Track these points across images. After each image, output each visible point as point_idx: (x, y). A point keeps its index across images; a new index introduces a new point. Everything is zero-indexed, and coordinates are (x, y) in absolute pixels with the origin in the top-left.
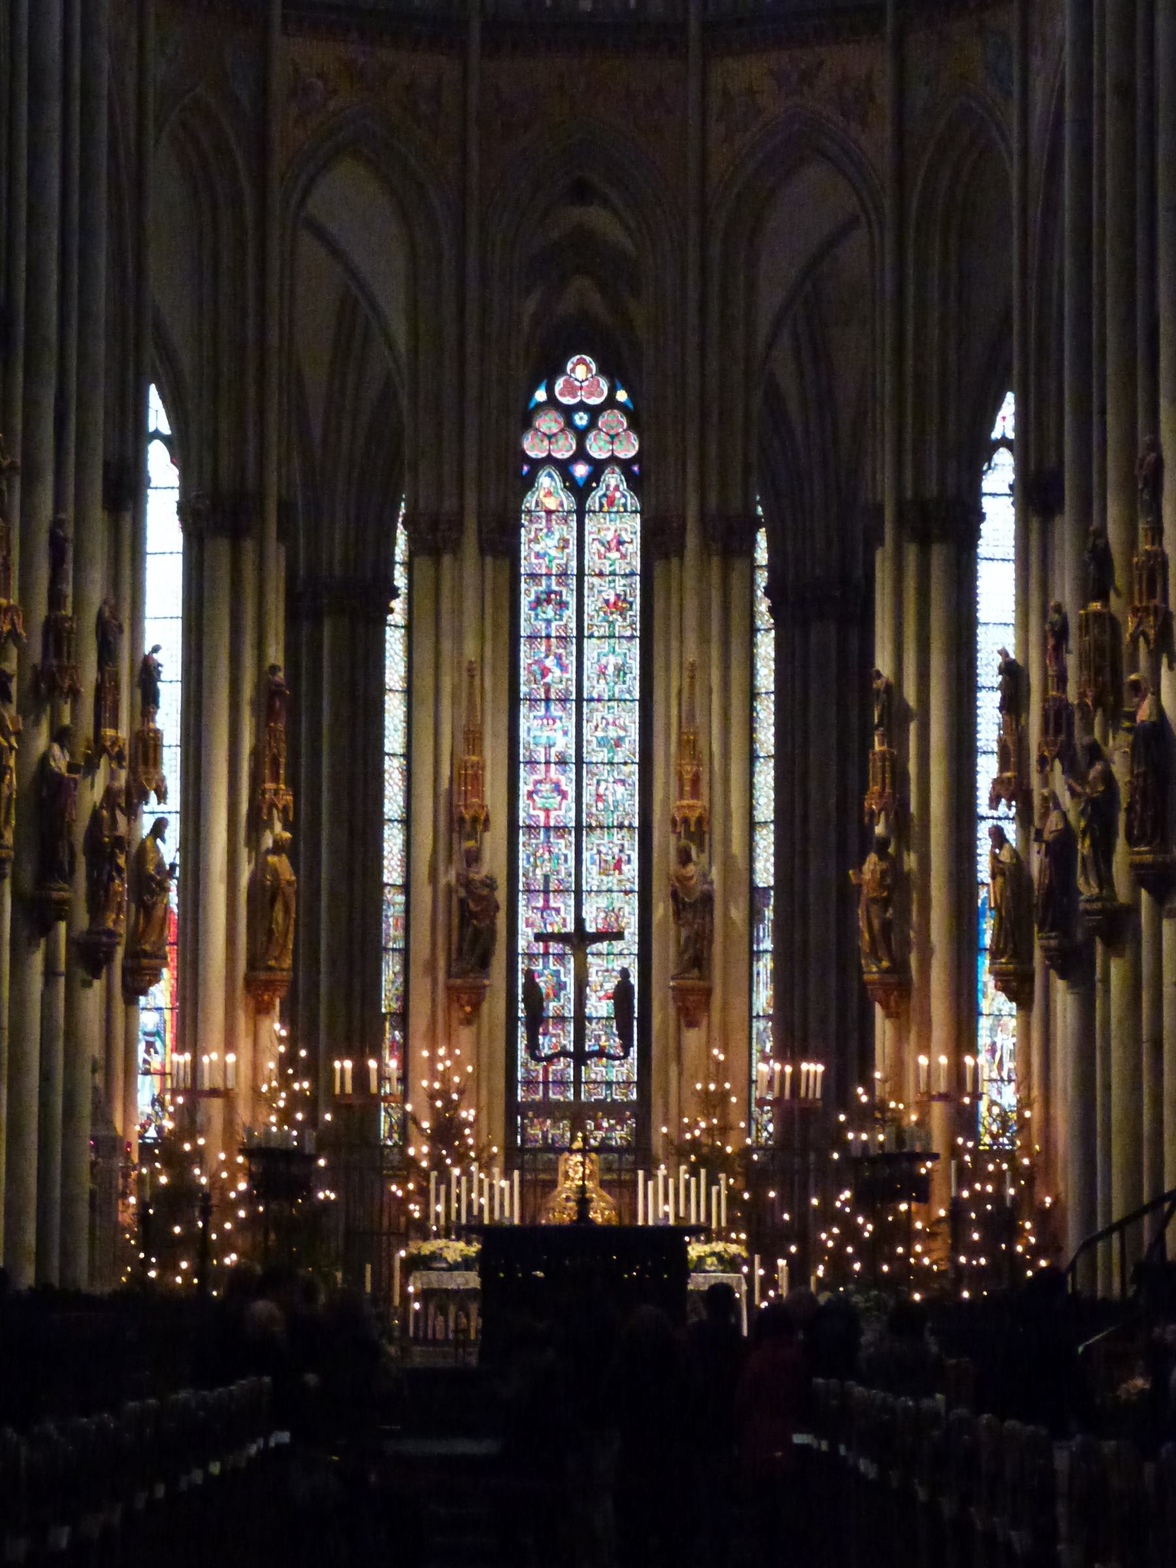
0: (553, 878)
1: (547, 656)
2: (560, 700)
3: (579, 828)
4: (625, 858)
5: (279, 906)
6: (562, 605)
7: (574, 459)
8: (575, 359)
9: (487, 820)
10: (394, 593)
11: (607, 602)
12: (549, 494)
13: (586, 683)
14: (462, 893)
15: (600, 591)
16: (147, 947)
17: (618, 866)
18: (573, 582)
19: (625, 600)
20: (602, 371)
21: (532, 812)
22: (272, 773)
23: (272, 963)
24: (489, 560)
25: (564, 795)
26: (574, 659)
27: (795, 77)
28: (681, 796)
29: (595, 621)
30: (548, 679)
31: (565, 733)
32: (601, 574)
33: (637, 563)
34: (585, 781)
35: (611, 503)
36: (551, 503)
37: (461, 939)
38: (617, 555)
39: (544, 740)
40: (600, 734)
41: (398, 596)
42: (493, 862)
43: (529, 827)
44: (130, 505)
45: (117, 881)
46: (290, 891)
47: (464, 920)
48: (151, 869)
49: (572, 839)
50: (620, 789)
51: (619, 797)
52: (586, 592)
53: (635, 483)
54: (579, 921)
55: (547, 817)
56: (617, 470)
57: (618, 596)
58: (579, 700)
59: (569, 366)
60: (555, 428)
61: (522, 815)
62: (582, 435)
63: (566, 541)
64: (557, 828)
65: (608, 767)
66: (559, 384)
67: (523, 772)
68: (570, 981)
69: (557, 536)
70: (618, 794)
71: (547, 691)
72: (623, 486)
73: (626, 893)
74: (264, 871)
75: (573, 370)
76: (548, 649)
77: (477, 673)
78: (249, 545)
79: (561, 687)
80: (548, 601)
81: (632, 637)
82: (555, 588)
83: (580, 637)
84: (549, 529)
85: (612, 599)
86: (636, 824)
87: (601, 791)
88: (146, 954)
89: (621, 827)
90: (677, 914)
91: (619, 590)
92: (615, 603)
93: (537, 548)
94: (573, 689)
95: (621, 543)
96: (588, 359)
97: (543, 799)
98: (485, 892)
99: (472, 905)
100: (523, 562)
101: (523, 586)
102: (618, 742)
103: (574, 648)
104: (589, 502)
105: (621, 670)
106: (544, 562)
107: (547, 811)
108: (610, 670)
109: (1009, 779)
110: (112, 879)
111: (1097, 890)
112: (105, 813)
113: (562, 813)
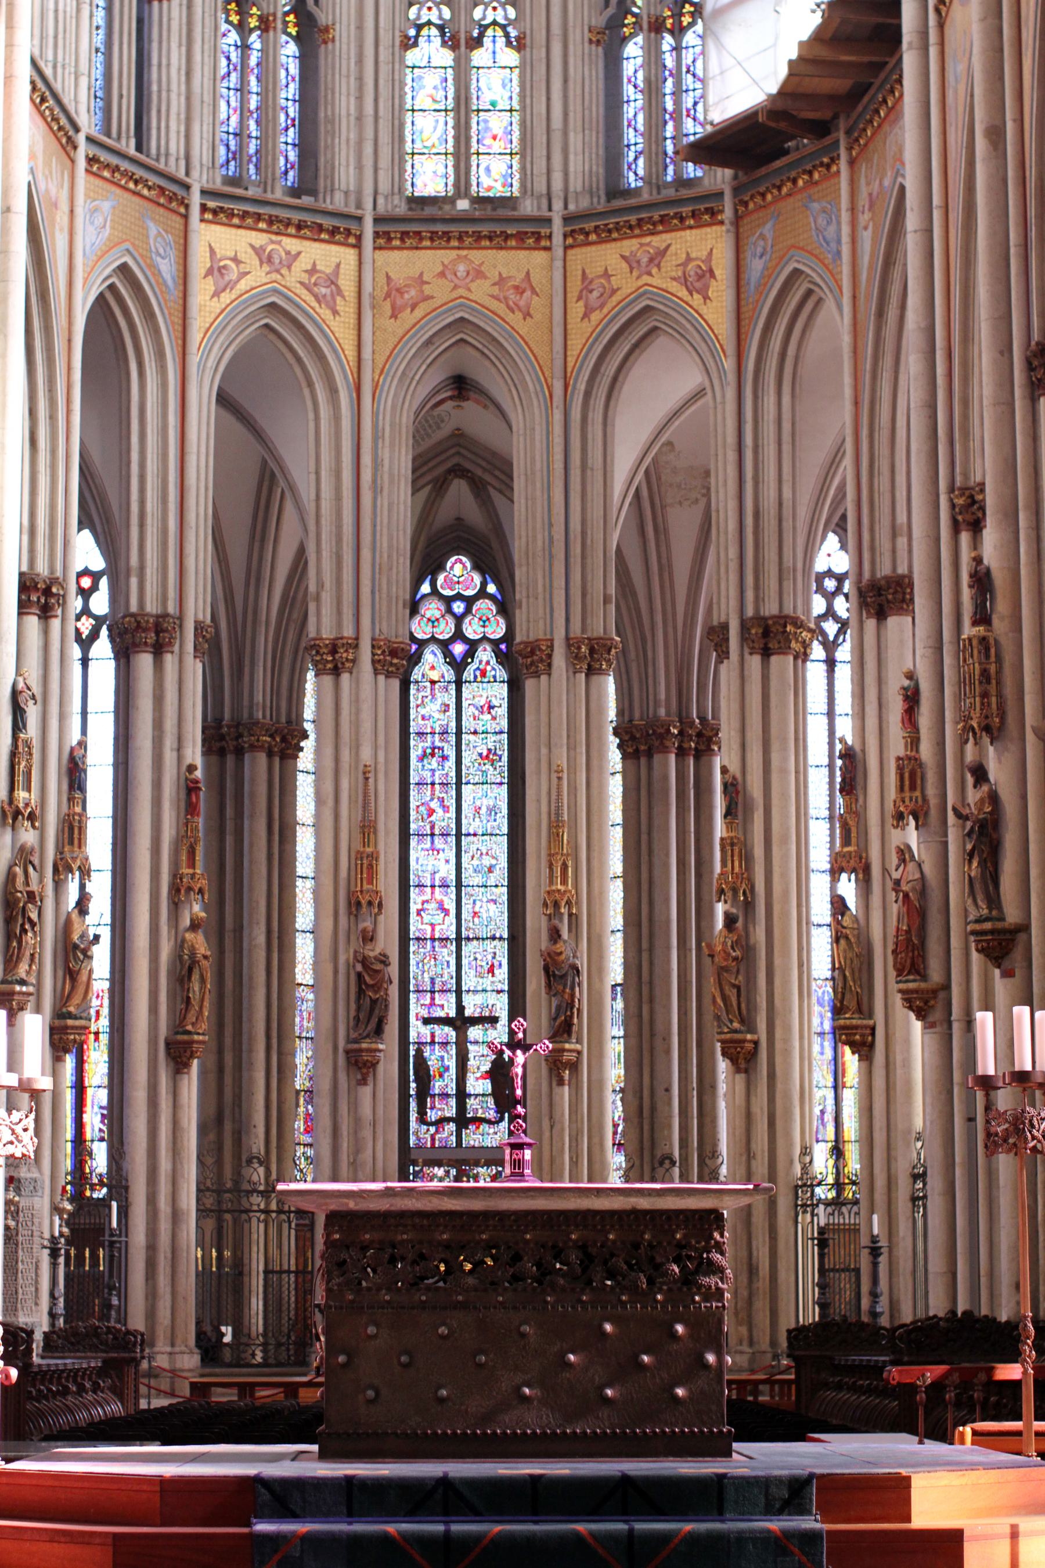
0: (438, 980)
1: (432, 799)
2: (443, 835)
3: (459, 939)
4: (496, 964)
5: (196, 977)
6: (445, 758)
7: (452, 640)
8: (453, 559)
9: (380, 905)
10: (305, 736)
11: (480, 755)
12: (433, 668)
13: (464, 821)
14: (359, 968)
15: (474, 747)
16: (72, 1009)
17: (491, 970)
18: (453, 739)
19: (495, 754)
20: (477, 567)
21: (420, 926)
22: (188, 859)
23: (189, 1028)
24: (381, 678)
25: (447, 912)
26: (454, 801)
27: (645, 260)
28: (551, 883)
29: (472, 771)
30: (432, 818)
31: (447, 861)
32: (475, 733)
33: (504, 724)
34: (464, 901)
35: (484, 674)
36: (434, 675)
37: (359, 1009)
38: (489, 717)
39: (430, 868)
40: (475, 862)
41: (307, 737)
42: (387, 942)
43: (418, 939)
44: (59, 612)
45: (30, 934)
46: (205, 963)
47: (360, 993)
48: (75, 937)
49: (453, 948)
50: (492, 906)
51: (491, 914)
52: (464, 747)
53: (503, 658)
54: (460, 1008)
55: (433, 930)
56: (488, 648)
57: (489, 750)
58: (459, 835)
59: (449, 565)
60: (438, 614)
61: (412, 929)
62: (459, 619)
63: (448, 706)
64: (441, 939)
65: (483, 889)
66: (441, 579)
67: (413, 893)
68: (452, 1064)
69: (439, 702)
70: (491, 912)
71: (432, 827)
72: (493, 661)
73: (499, 992)
74: (182, 947)
75: (452, 568)
76: (433, 794)
77: (371, 775)
78: (170, 660)
79: (443, 824)
80: (433, 755)
81: (501, 784)
82: (438, 744)
83: (459, 784)
84: (433, 696)
85: (485, 753)
86: (506, 936)
87: (477, 909)
88: (70, 1016)
89: (493, 938)
90: (549, 986)
91: (491, 746)
92: (487, 757)
93: (422, 711)
94: (453, 826)
95: (491, 707)
96: (464, 559)
97: (428, 917)
98: (378, 966)
99: (367, 978)
100: (412, 723)
101: (412, 743)
102: (490, 870)
103: (454, 793)
104: (465, 674)
105: (492, 810)
106: (429, 723)
107: (433, 926)
108: (483, 811)
109: (850, 853)
110: (24, 931)
111: (986, 911)
112: (17, 869)
113: (444, 927)
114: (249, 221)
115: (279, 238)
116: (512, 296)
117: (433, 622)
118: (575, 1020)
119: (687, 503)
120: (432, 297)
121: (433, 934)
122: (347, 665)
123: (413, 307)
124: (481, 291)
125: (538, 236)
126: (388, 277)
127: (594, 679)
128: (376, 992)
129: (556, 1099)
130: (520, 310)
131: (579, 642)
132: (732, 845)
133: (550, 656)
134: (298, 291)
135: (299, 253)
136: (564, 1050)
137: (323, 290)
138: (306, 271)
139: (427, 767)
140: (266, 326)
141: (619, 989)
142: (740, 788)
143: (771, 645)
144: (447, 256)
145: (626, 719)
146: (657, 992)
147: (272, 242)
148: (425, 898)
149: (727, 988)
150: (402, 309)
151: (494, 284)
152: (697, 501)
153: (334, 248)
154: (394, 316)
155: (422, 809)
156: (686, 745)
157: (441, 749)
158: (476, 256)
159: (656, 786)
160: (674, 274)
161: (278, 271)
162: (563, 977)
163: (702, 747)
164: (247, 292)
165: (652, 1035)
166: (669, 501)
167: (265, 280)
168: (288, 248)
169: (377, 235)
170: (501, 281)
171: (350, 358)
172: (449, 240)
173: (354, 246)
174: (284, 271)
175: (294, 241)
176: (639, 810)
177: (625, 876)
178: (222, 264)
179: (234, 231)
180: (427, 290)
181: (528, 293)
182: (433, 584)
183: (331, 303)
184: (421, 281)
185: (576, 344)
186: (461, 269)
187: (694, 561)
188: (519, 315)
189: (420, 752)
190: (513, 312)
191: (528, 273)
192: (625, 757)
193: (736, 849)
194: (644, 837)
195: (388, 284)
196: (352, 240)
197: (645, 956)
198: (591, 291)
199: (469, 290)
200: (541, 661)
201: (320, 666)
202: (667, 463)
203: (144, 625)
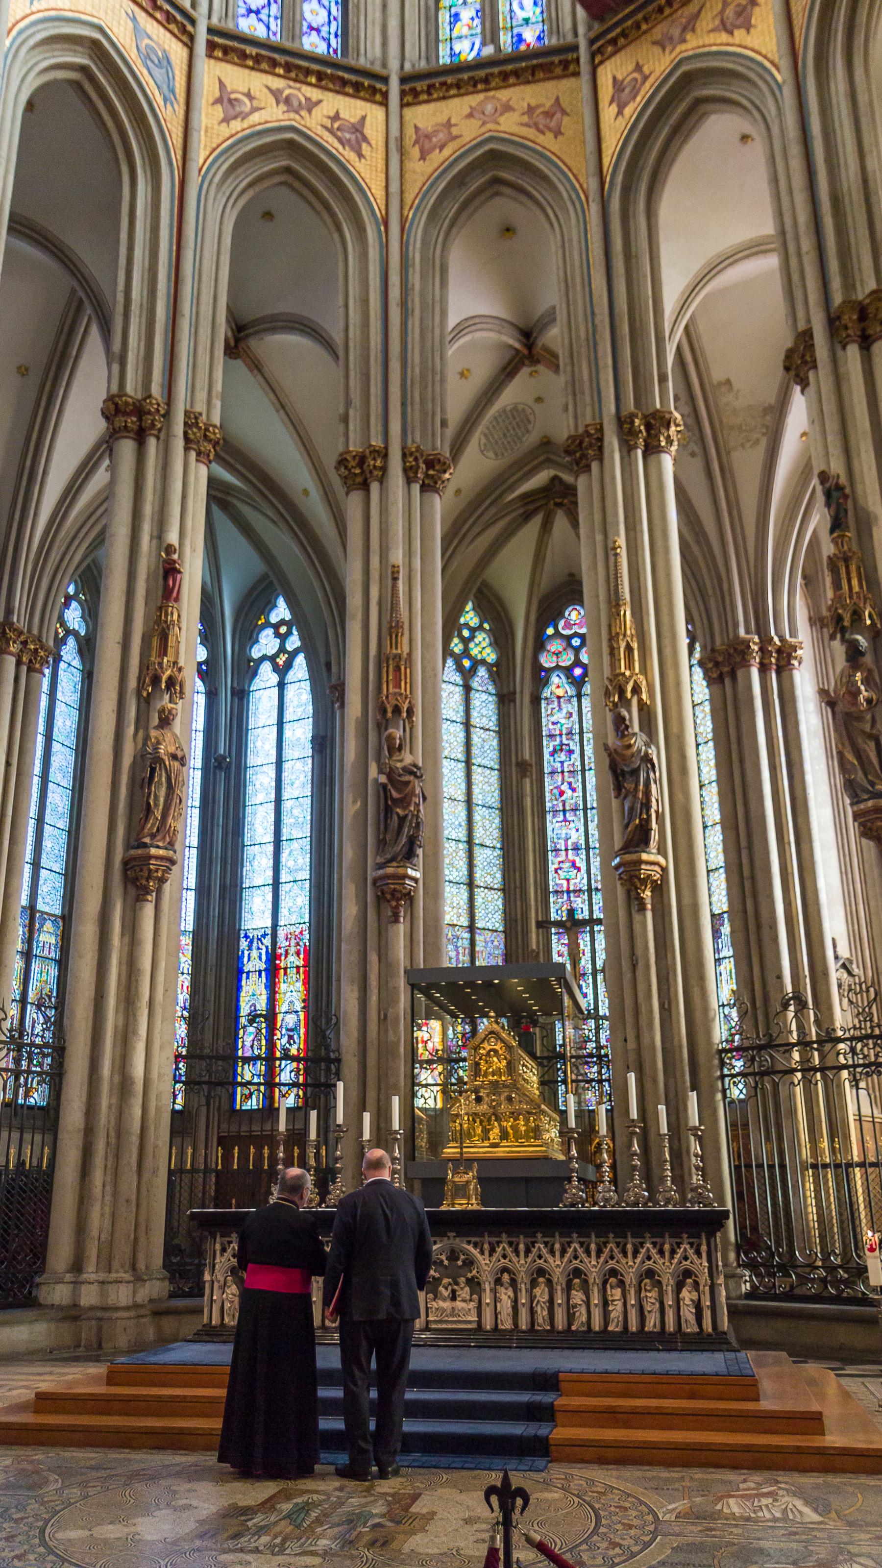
6: (571, 752)
8: (570, 608)
18: (577, 738)
25: (579, 869)
30: (563, 798)
31: (577, 830)
36: (560, 692)
39: (563, 836)
43: (556, 892)
47: (388, 810)
49: (586, 897)
59: (567, 613)
61: (551, 883)
64: (575, 891)
66: (561, 624)
69: (565, 711)
71: (564, 805)
80: (561, 750)
82: (565, 741)
94: (581, 803)
101: (545, 743)
104: (584, 689)
107: (568, 880)
113: (577, 881)
114: (264, 66)
115: (298, 85)
116: (542, 121)
117: (557, 654)
118: (654, 825)
119: (748, 445)
120: (461, 136)
121: (568, 888)
122: (375, 473)
123: (442, 148)
124: (510, 124)
125: (565, 64)
126: (416, 127)
127: (652, 459)
128: (405, 808)
129: (637, 927)
130: (550, 130)
131: (632, 417)
132: (846, 560)
133: (601, 440)
134: (319, 132)
135: (320, 101)
136: (641, 862)
137: (348, 136)
138: (329, 117)
139: (558, 759)
140: (288, 170)
141: (725, 916)
142: (848, 491)
143: (870, 332)
144: (474, 100)
145: (709, 648)
146: (760, 883)
147: (290, 87)
148: (559, 859)
149: (860, 740)
150: (432, 150)
151: (523, 114)
152: (757, 441)
153: (359, 103)
154: (423, 158)
155: (556, 791)
156: (766, 661)
157: (568, 745)
158: (504, 95)
159: (741, 697)
160: (711, 27)
161: (297, 112)
162: (635, 772)
163: (782, 663)
164: (260, 124)
165: (759, 927)
166: (732, 444)
167: (281, 117)
168: (308, 95)
169: (403, 93)
170: (530, 110)
171: (378, 197)
172: (475, 86)
173: (380, 104)
174: (303, 113)
175: (315, 90)
176: (727, 727)
177: (723, 823)
178: (233, 96)
179: (247, 71)
180: (455, 131)
181: (558, 115)
182: (556, 628)
183: (357, 147)
184: (449, 124)
185: (611, 144)
186: (489, 108)
187: (760, 499)
188: (550, 135)
189: (551, 749)
190: (543, 133)
191: (557, 99)
192: (710, 681)
193: (853, 568)
194: (734, 747)
195: (416, 133)
196: (378, 97)
197: (744, 853)
198: (623, 90)
199: (498, 124)
200: (591, 445)
201: (350, 482)
202: (727, 404)
203: (122, 408)
